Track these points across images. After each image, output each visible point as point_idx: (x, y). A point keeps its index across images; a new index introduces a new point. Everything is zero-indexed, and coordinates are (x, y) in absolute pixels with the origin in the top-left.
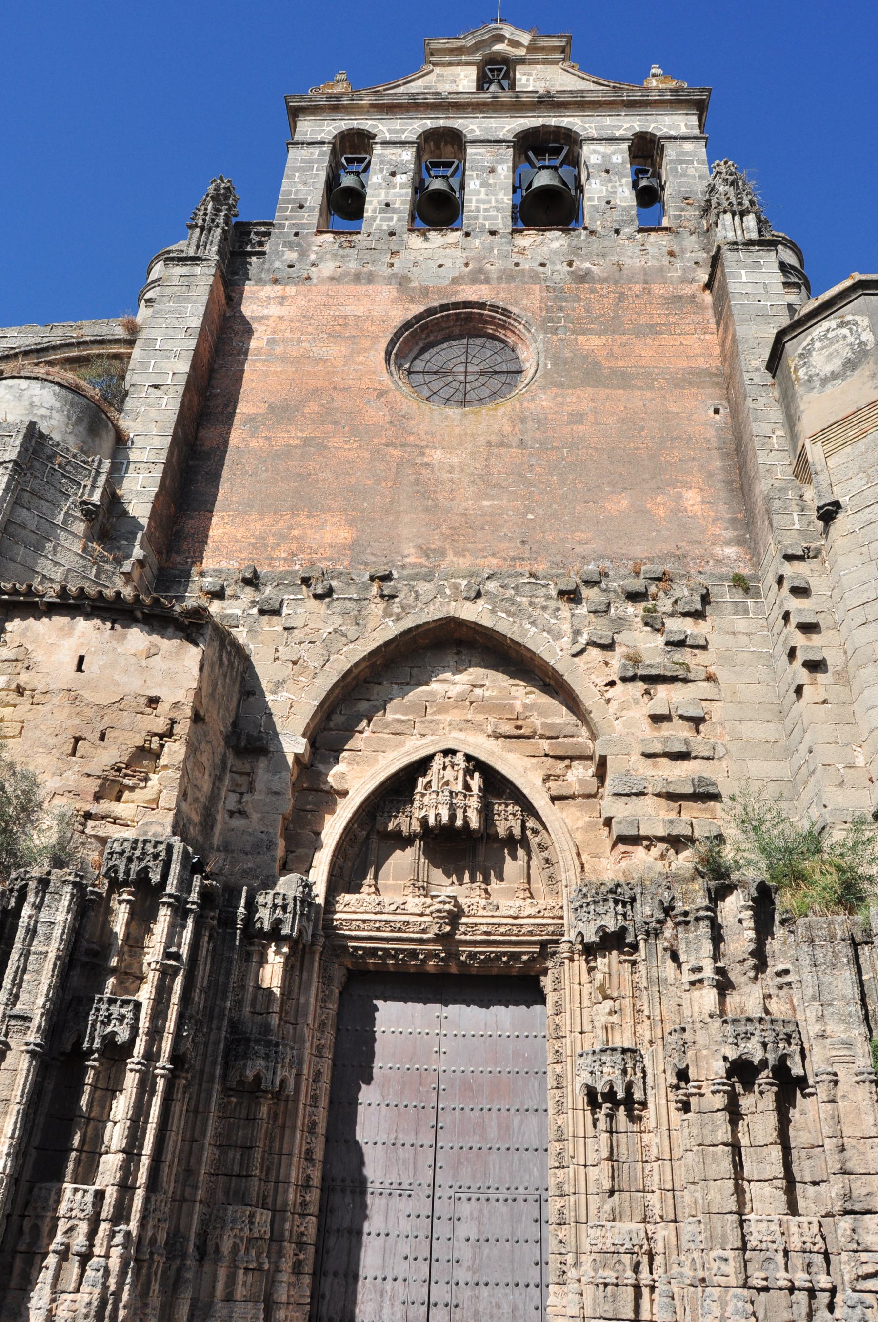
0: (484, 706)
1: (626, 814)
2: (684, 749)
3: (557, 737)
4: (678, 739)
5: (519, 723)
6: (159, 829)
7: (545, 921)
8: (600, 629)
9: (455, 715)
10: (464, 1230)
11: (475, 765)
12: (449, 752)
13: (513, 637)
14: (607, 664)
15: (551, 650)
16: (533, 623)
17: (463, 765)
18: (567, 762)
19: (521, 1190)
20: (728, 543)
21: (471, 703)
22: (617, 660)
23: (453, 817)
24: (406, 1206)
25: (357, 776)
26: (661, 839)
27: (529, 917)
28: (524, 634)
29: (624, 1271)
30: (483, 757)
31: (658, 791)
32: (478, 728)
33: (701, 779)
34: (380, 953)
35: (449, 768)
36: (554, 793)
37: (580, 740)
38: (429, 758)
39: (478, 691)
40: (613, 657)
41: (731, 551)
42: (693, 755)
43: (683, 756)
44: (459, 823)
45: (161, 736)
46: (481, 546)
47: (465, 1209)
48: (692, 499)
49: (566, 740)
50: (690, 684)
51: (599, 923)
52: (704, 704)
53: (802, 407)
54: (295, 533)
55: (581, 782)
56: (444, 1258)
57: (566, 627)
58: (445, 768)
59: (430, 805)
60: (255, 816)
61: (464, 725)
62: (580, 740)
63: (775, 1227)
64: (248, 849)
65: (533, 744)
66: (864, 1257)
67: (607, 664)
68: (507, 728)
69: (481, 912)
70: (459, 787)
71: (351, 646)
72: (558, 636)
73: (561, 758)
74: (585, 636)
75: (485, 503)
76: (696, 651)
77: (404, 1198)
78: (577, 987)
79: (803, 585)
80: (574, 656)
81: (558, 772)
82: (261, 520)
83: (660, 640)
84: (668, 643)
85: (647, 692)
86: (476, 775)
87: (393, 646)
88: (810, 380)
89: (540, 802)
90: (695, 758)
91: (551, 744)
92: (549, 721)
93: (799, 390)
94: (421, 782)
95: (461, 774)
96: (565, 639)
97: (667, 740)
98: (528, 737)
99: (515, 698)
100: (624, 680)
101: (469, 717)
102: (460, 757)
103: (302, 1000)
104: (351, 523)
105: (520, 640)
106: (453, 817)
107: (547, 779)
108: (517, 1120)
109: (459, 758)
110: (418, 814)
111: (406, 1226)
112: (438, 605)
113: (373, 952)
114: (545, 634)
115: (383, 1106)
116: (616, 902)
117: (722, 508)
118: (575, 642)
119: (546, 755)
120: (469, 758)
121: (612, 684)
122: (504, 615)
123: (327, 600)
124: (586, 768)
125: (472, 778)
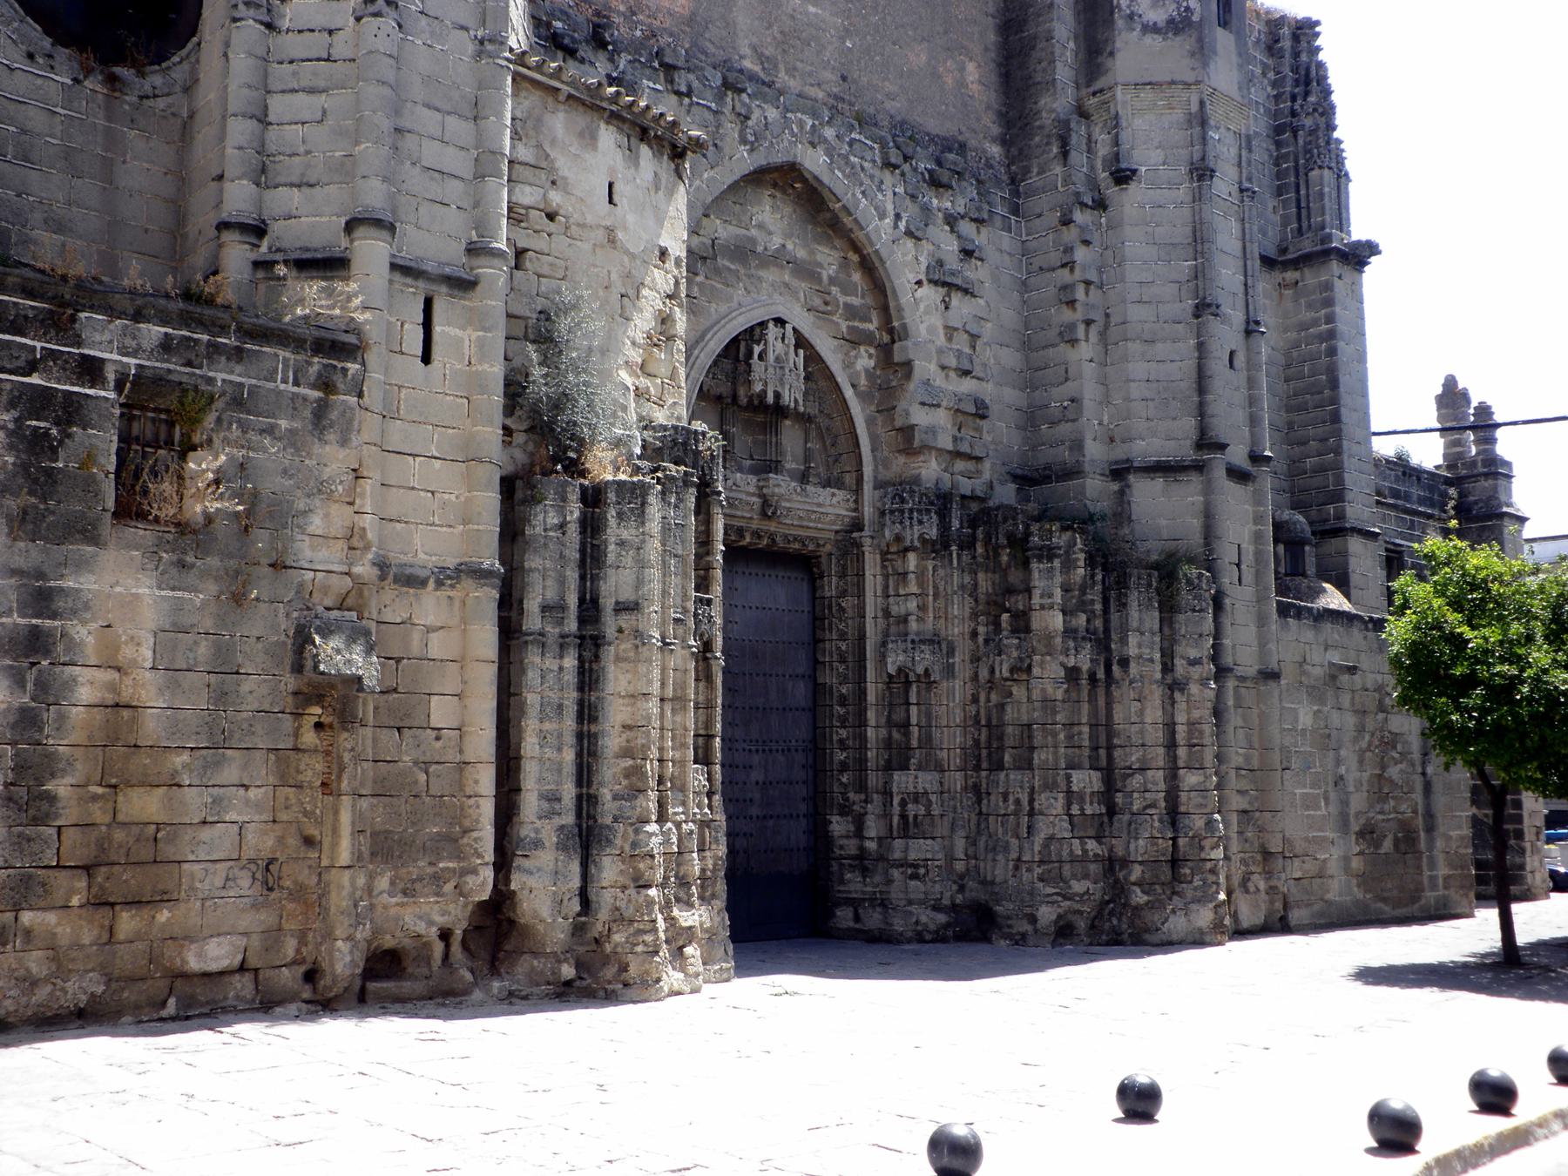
12: (780, 322)
15: (877, 229)
38: (763, 325)
41: (995, 150)
46: (809, 68)
48: (972, 72)
53: (1118, 44)
57: (890, 207)
68: (817, 302)
71: (712, 173)
72: (882, 216)
75: (812, 9)
86: (801, 352)
88: (1131, 17)
93: (1120, 23)
108: (790, 685)
110: (758, 387)
112: (786, 143)
117: (993, 95)
121: (919, 283)
123: (686, 101)
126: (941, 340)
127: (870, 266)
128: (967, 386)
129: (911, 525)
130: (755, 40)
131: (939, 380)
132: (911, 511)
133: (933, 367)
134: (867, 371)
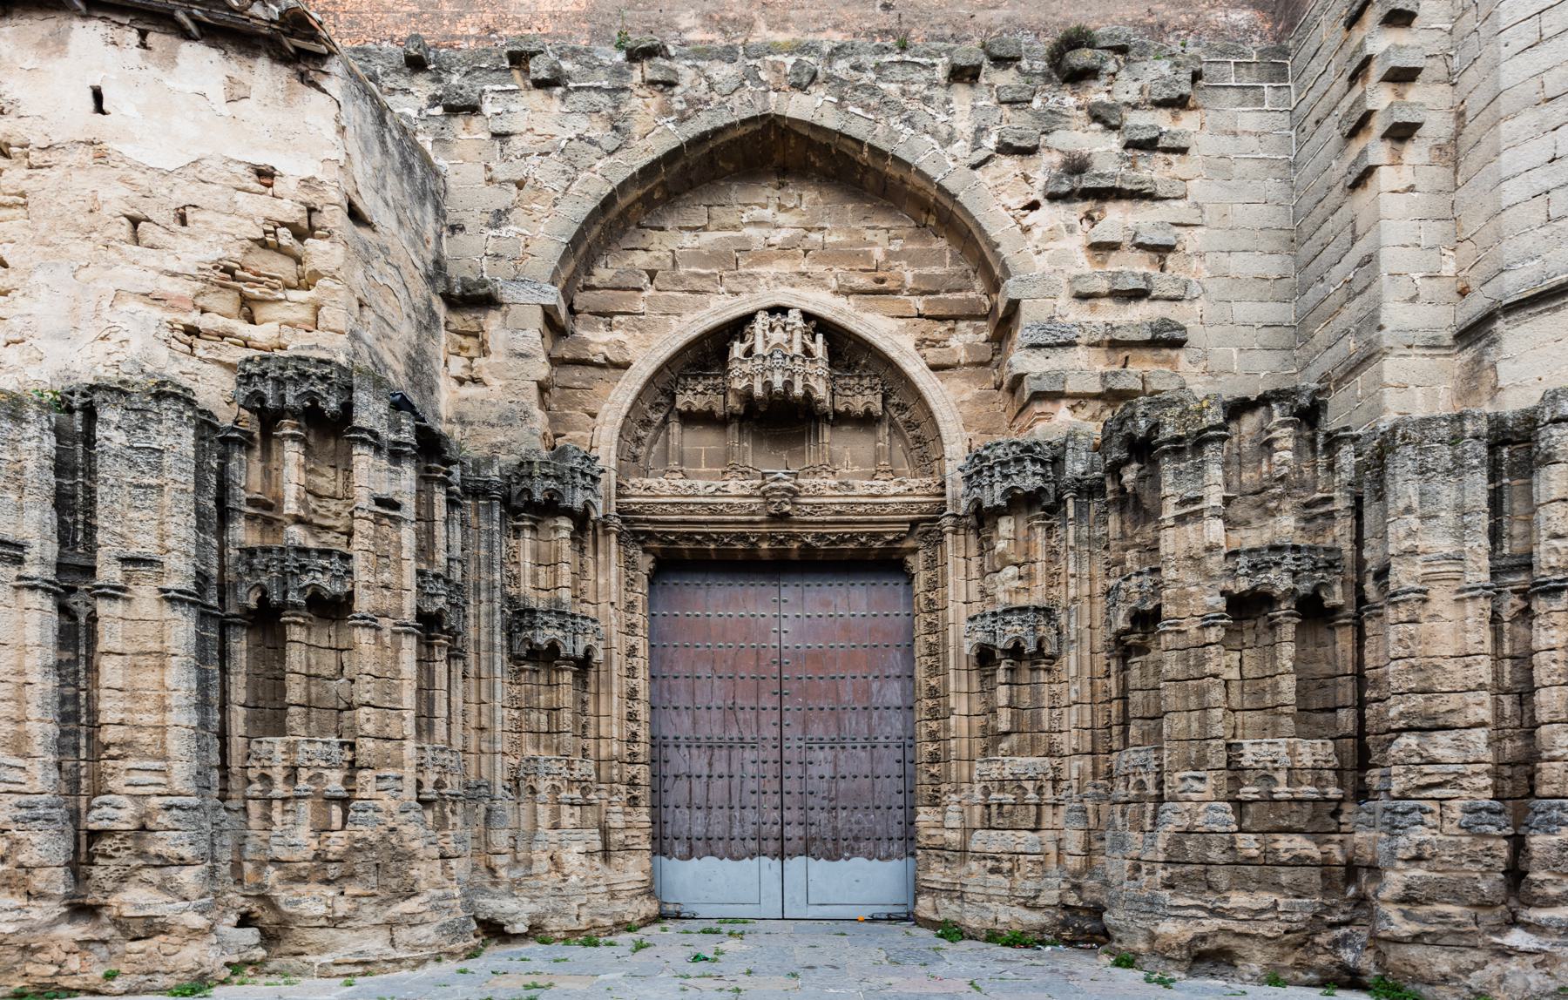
1: (1047, 368)
2: (1143, 286)
3: (937, 292)
4: (1133, 275)
5: (880, 275)
7: (917, 499)
8: (1017, 124)
11: (816, 323)
13: (875, 143)
14: (1026, 178)
16: (908, 121)
17: (800, 324)
18: (950, 324)
21: (806, 252)
22: (1043, 169)
23: (789, 384)
26: (1097, 397)
27: (895, 495)
28: (893, 136)
30: (827, 313)
31: (1097, 338)
32: (820, 282)
33: (1165, 322)
35: (779, 329)
36: (932, 361)
37: (971, 295)
39: (816, 236)
40: (1037, 168)
42: (1154, 294)
43: (1138, 295)
44: (798, 391)
49: (949, 296)
50: (1157, 204)
52: (1177, 230)
55: (970, 348)
58: (772, 329)
61: (796, 279)
62: (971, 295)
65: (901, 302)
66: (1427, 769)
67: (1026, 178)
68: (862, 281)
69: (829, 492)
73: (941, 319)
74: (994, 138)
81: (938, 336)
84: (1131, 145)
85: (1088, 216)
86: (820, 337)
89: (915, 368)
92: (926, 271)
94: (737, 349)
95: (797, 334)
96: (961, 143)
97: (1115, 276)
98: (894, 292)
99: (872, 244)
100: (1053, 197)
101: (803, 269)
102: (794, 317)
105: (885, 147)
106: (789, 384)
107: (921, 343)
109: (794, 317)
114: (927, 137)
118: (976, 145)
120: (807, 316)
124: (977, 330)
125: (814, 340)
127: (938, 214)
129: (991, 486)
131: (1075, 314)
132: (991, 468)
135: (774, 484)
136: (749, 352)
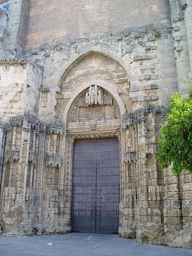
0: (102, 72)
3: (120, 78)
4: (148, 75)
5: (111, 76)
6: (21, 113)
9: (94, 76)
10: (103, 192)
15: (116, 56)
19: (115, 183)
20: (164, 19)
23: (94, 102)
24: (90, 188)
25: (71, 94)
28: (109, 52)
29: (130, 198)
33: (153, 85)
34: (80, 135)
35: (93, 90)
43: (149, 79)
44: (96, 103)
45: (20, 92)
47: (103, 188)
51: (126, 124)
54: (53, 35)
56: (99, 198)
57: (120, 49)
58: (92, 90)
59: (89, 99)
60: (48, 107)
63: (154, 188)
64: (47, 115)
67: (130, 57)
68: (107, 78)
70: (96, 94)
72: (118, 52)
74: (125, 51)
75: (100, 18)
76: (154, 51)
77: (90, 187)
78: (124, 139)
79: (178, 29)
80: (122, 56)
82: (45, 33)
83: (144, 49)
87: (78, 60)
89: (116, 96)
90: (152, 79)
91: (119, 80)
92: (118, 74)
94: (87, 94)
95: (96, 90)
102: (96, 86)
103: (63, 147)
104: (67, 30)
106: (94, 102)
109: (96, 86)
111: (90, 192)
113: (79, 135)
115: (84, 168)
116: (130, 118)
119: (118, 83)
121: (132, 62)
122: (104, 48)
126: (140, 73)
128: (150, 82)
130: (84, 31)
133: (137, 81)
134: (126, 89)
135: (92, 123)
136: (89, 95)
